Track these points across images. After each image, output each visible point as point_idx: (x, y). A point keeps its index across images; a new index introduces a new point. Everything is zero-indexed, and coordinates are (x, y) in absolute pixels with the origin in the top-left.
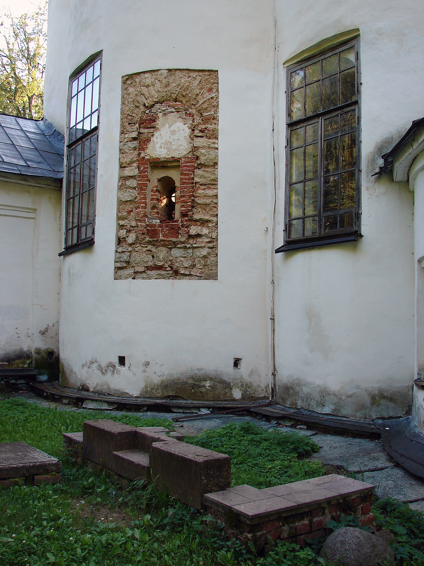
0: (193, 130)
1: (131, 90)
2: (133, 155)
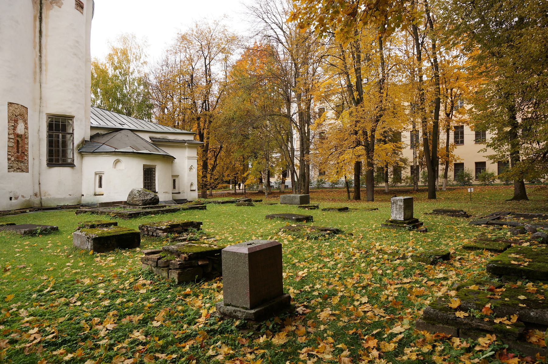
1: (11, 108)
2: (12, 132)
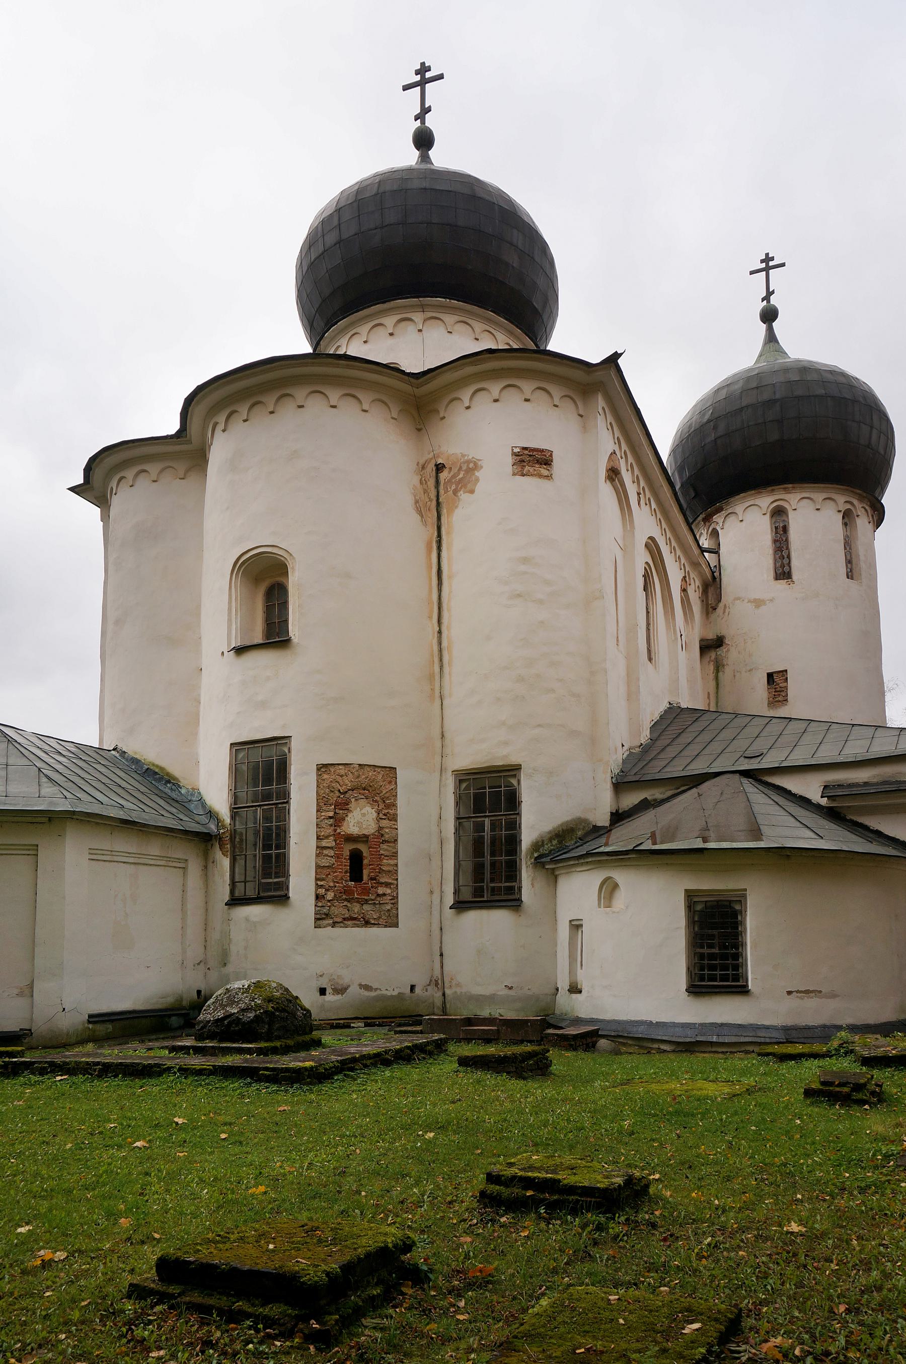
0: (378, 814)
1: (325, 776)
2: (330, 831)
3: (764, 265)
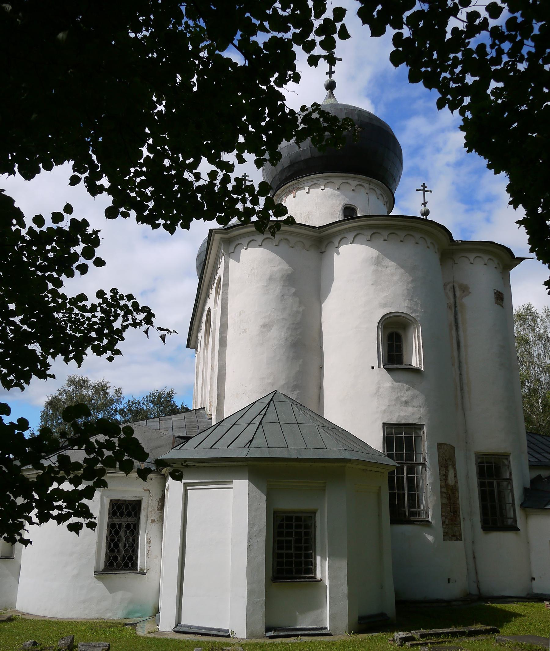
3: (422, 188)
